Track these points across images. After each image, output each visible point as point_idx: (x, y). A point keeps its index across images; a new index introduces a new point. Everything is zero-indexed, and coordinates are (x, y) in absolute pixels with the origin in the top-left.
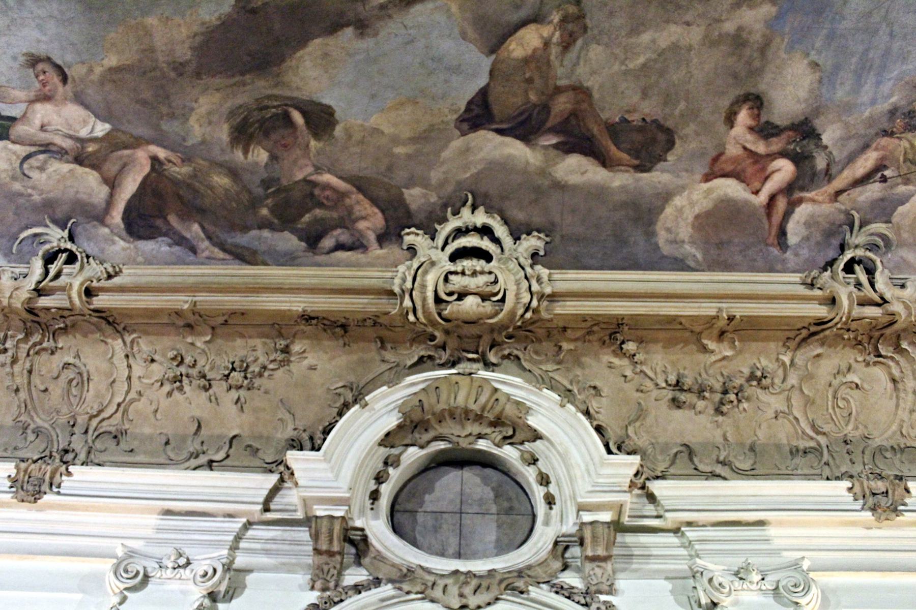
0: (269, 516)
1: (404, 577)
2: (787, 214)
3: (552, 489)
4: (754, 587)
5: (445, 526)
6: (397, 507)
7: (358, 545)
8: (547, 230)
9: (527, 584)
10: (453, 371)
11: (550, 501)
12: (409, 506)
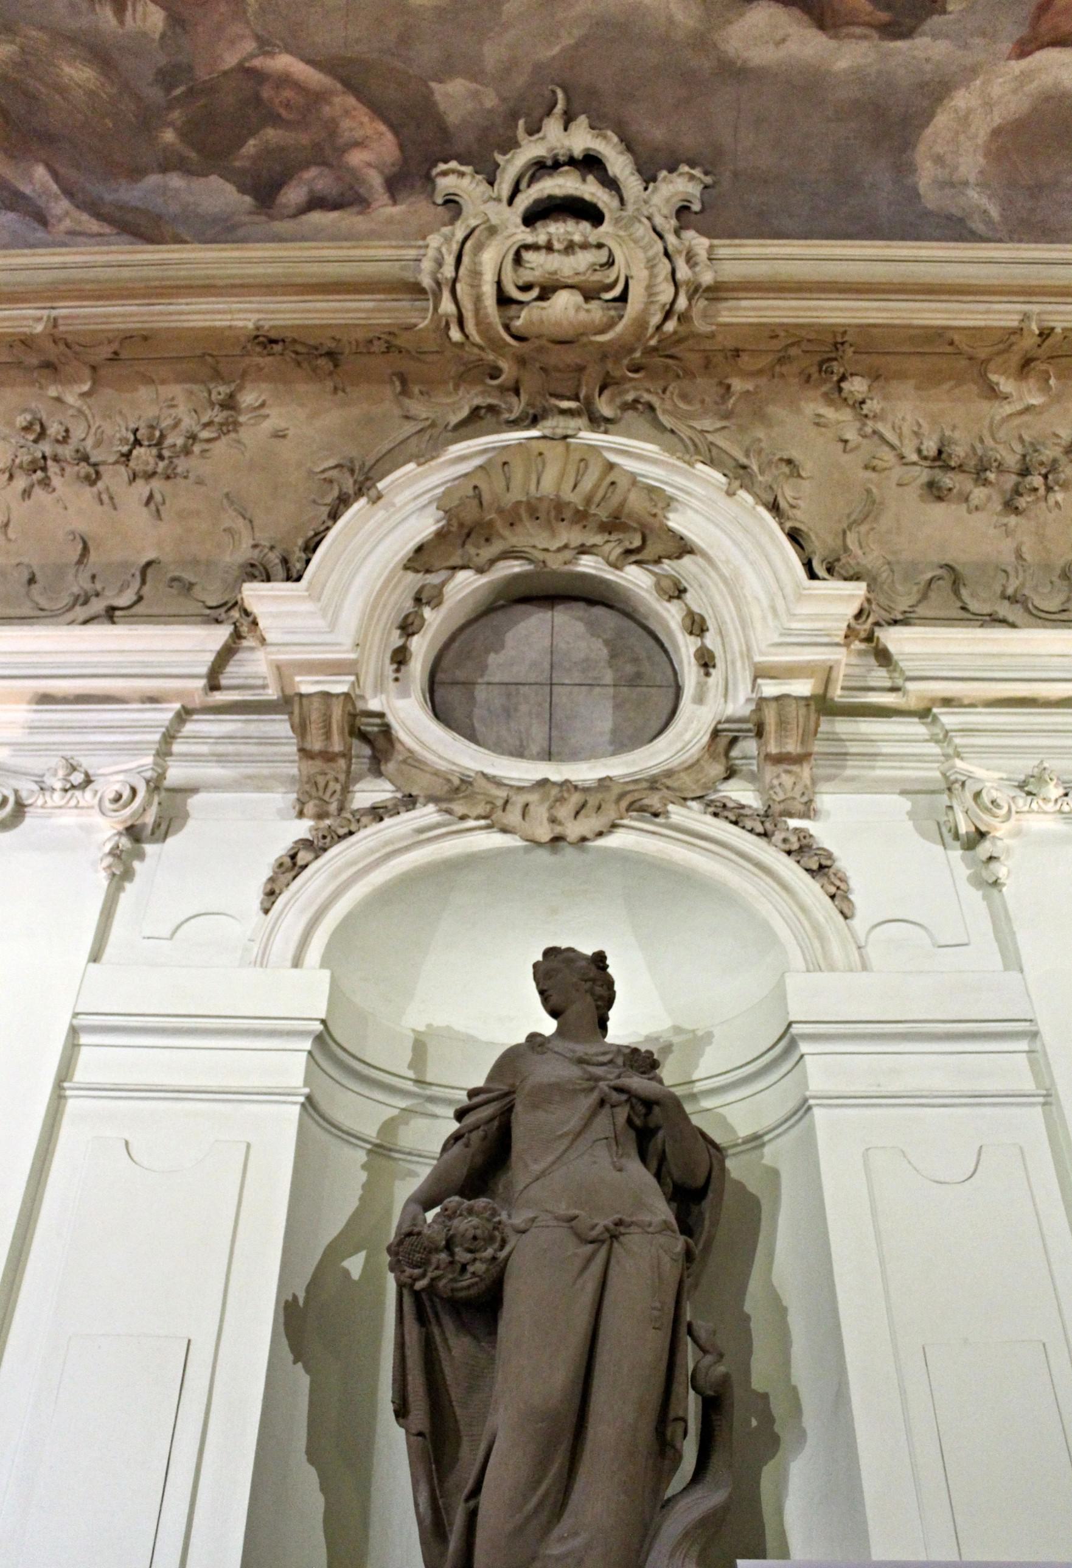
0: (219, 697)
1: (455, 792)
3: (711, 640)
4: (1050, 807)
5: (524, 708)
6: (440, 676)
7: (375, 741)
8: (706, 160)
9: (665, 802)
10: (534, 433)
12: (460, 675)
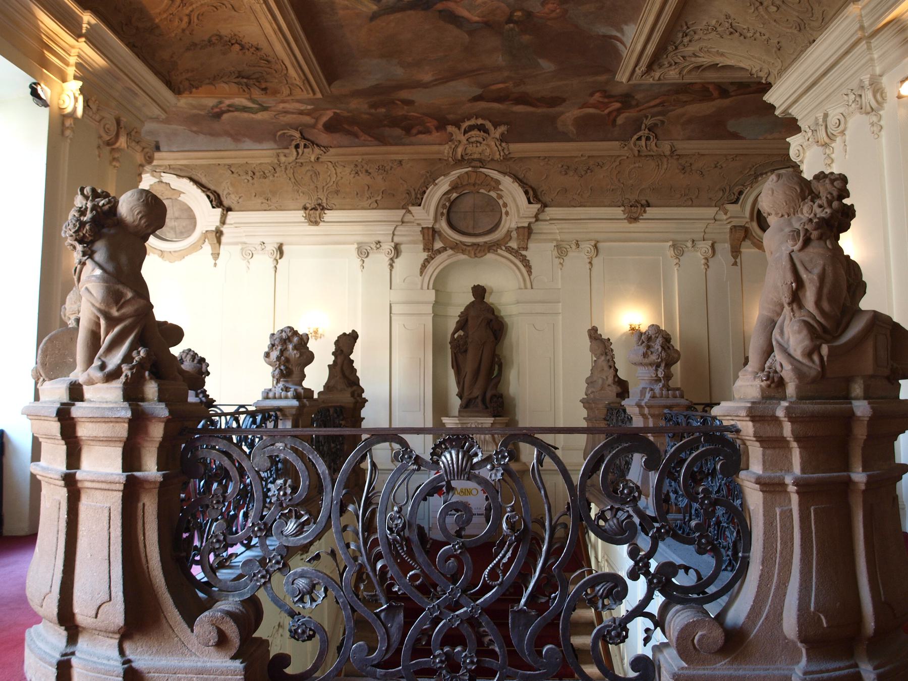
2: (616, 117)
10: (470, 169)
11: (507, 213)
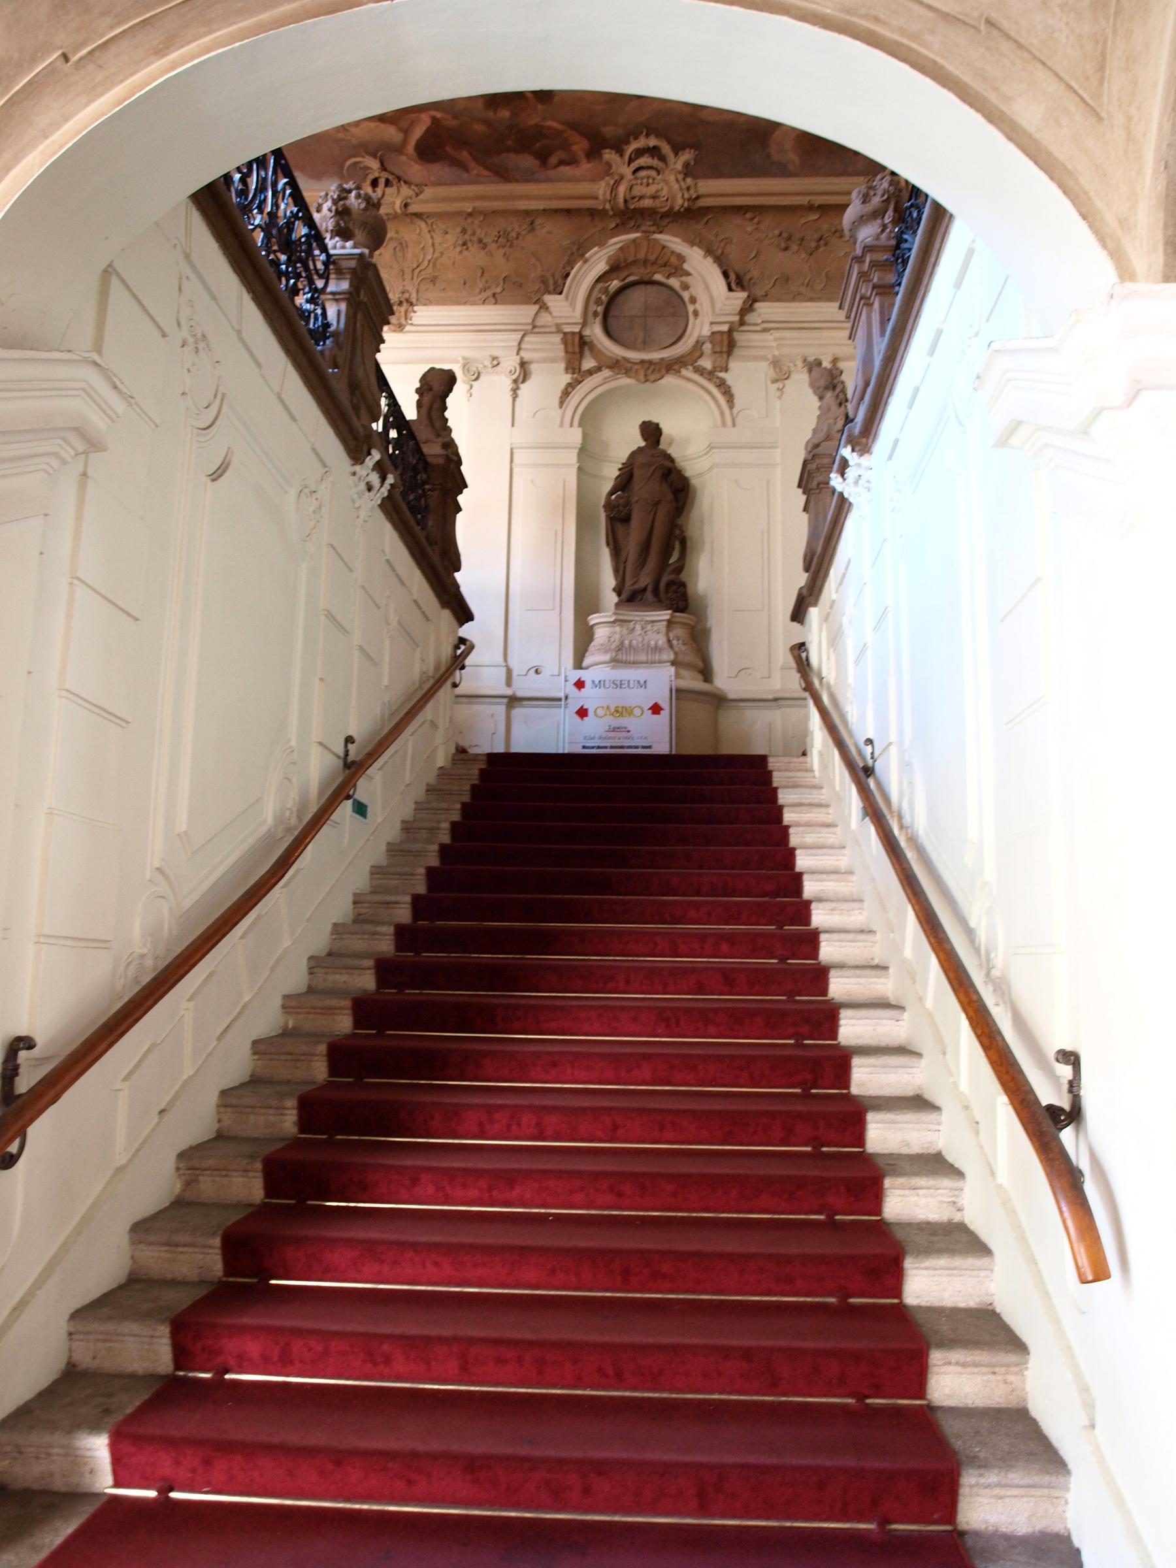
3: (697, 306)
8: (695, 146)
10: (638, 235)
11: (696, 313)
